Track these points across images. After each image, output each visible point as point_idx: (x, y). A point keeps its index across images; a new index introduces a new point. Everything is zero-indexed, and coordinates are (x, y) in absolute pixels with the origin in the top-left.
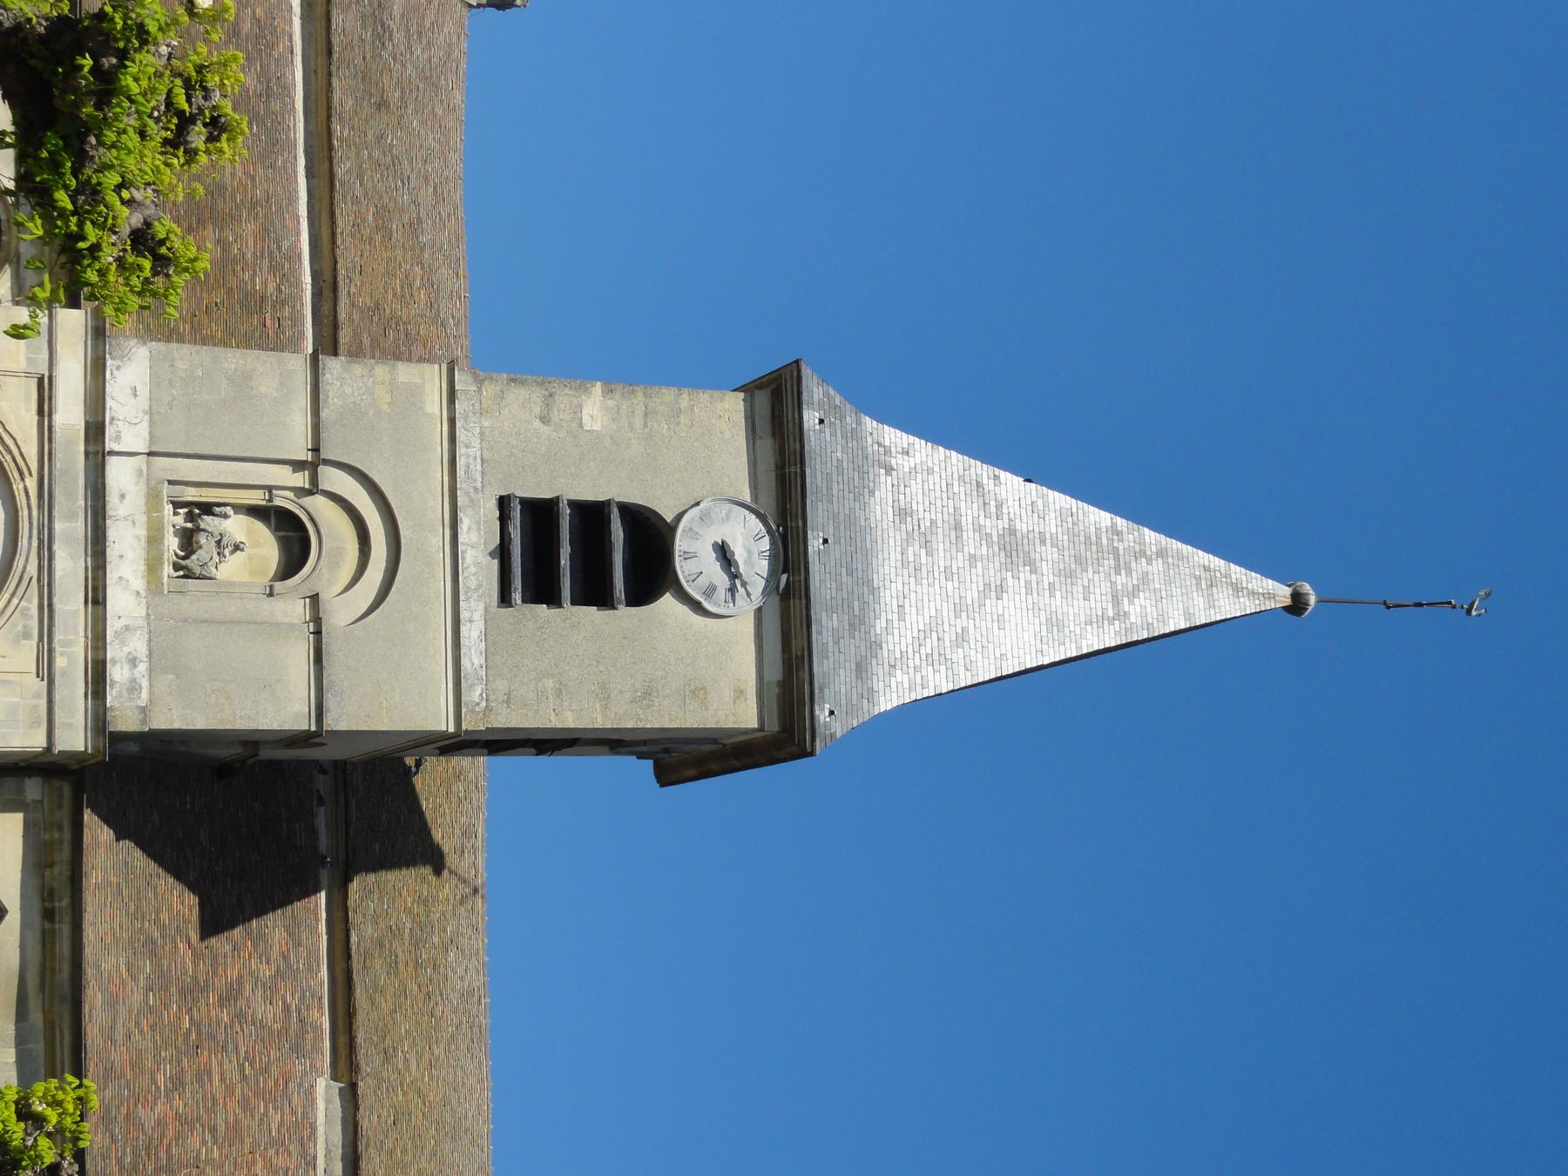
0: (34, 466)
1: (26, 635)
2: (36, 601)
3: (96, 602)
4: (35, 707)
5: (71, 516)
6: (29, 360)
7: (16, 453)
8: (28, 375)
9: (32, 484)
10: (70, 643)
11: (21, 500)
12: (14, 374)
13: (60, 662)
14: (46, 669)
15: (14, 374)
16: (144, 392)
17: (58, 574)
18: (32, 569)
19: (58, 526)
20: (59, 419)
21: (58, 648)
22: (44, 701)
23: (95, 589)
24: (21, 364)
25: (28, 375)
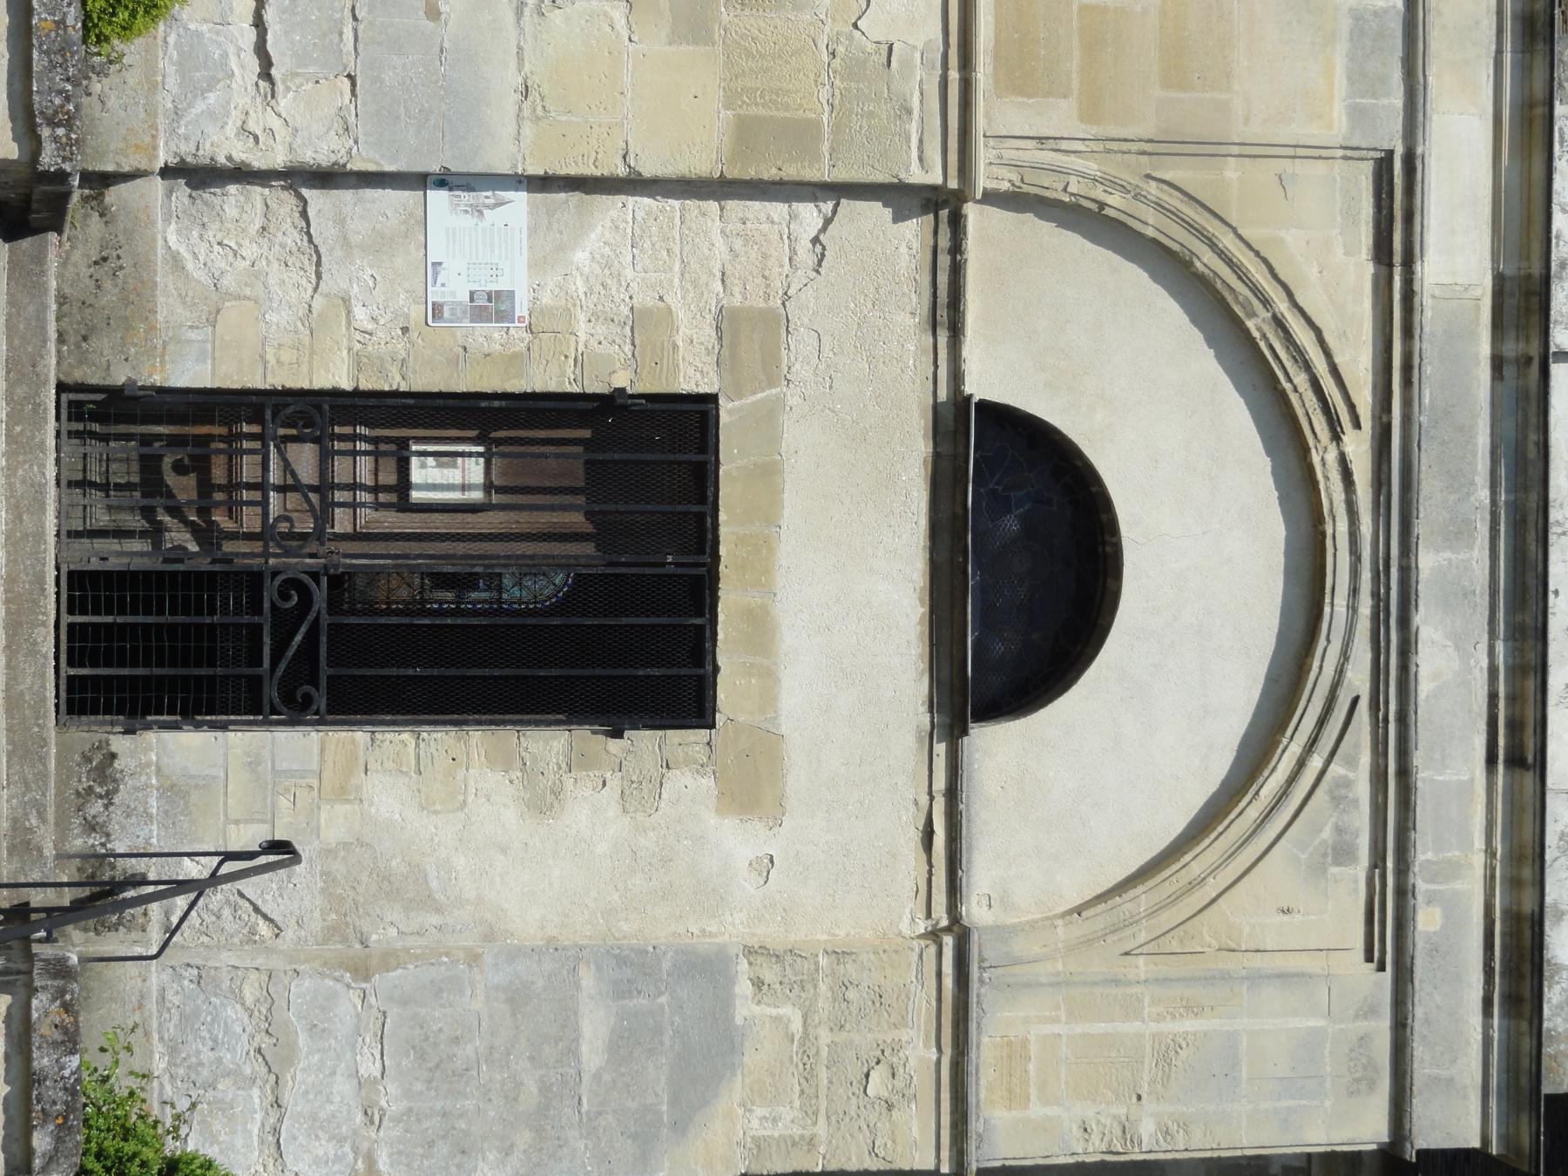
0: (1365, 401)
1: (1343, 853)
2: (1365, 759)
3: (1516, 761)
4: (1364, 1039)
5: (1457, 534)
6: (1357, 114)
7: (1321, 367)
8: (1351, 152)
9: (1358, 447)
10: (1452, 870)
12: (1317, 152)
13: (1427, 920)
14: (1390, 938)
15: (1317, 152)
17: (1425, 687)
18: (1358, 678)
19: (1427, 561)
20: (1433, 271)
21: (1421, 885)
22: (1383, 1026)
23: (1515, 726)
24: (1336, 126)
25: (1351, 152)
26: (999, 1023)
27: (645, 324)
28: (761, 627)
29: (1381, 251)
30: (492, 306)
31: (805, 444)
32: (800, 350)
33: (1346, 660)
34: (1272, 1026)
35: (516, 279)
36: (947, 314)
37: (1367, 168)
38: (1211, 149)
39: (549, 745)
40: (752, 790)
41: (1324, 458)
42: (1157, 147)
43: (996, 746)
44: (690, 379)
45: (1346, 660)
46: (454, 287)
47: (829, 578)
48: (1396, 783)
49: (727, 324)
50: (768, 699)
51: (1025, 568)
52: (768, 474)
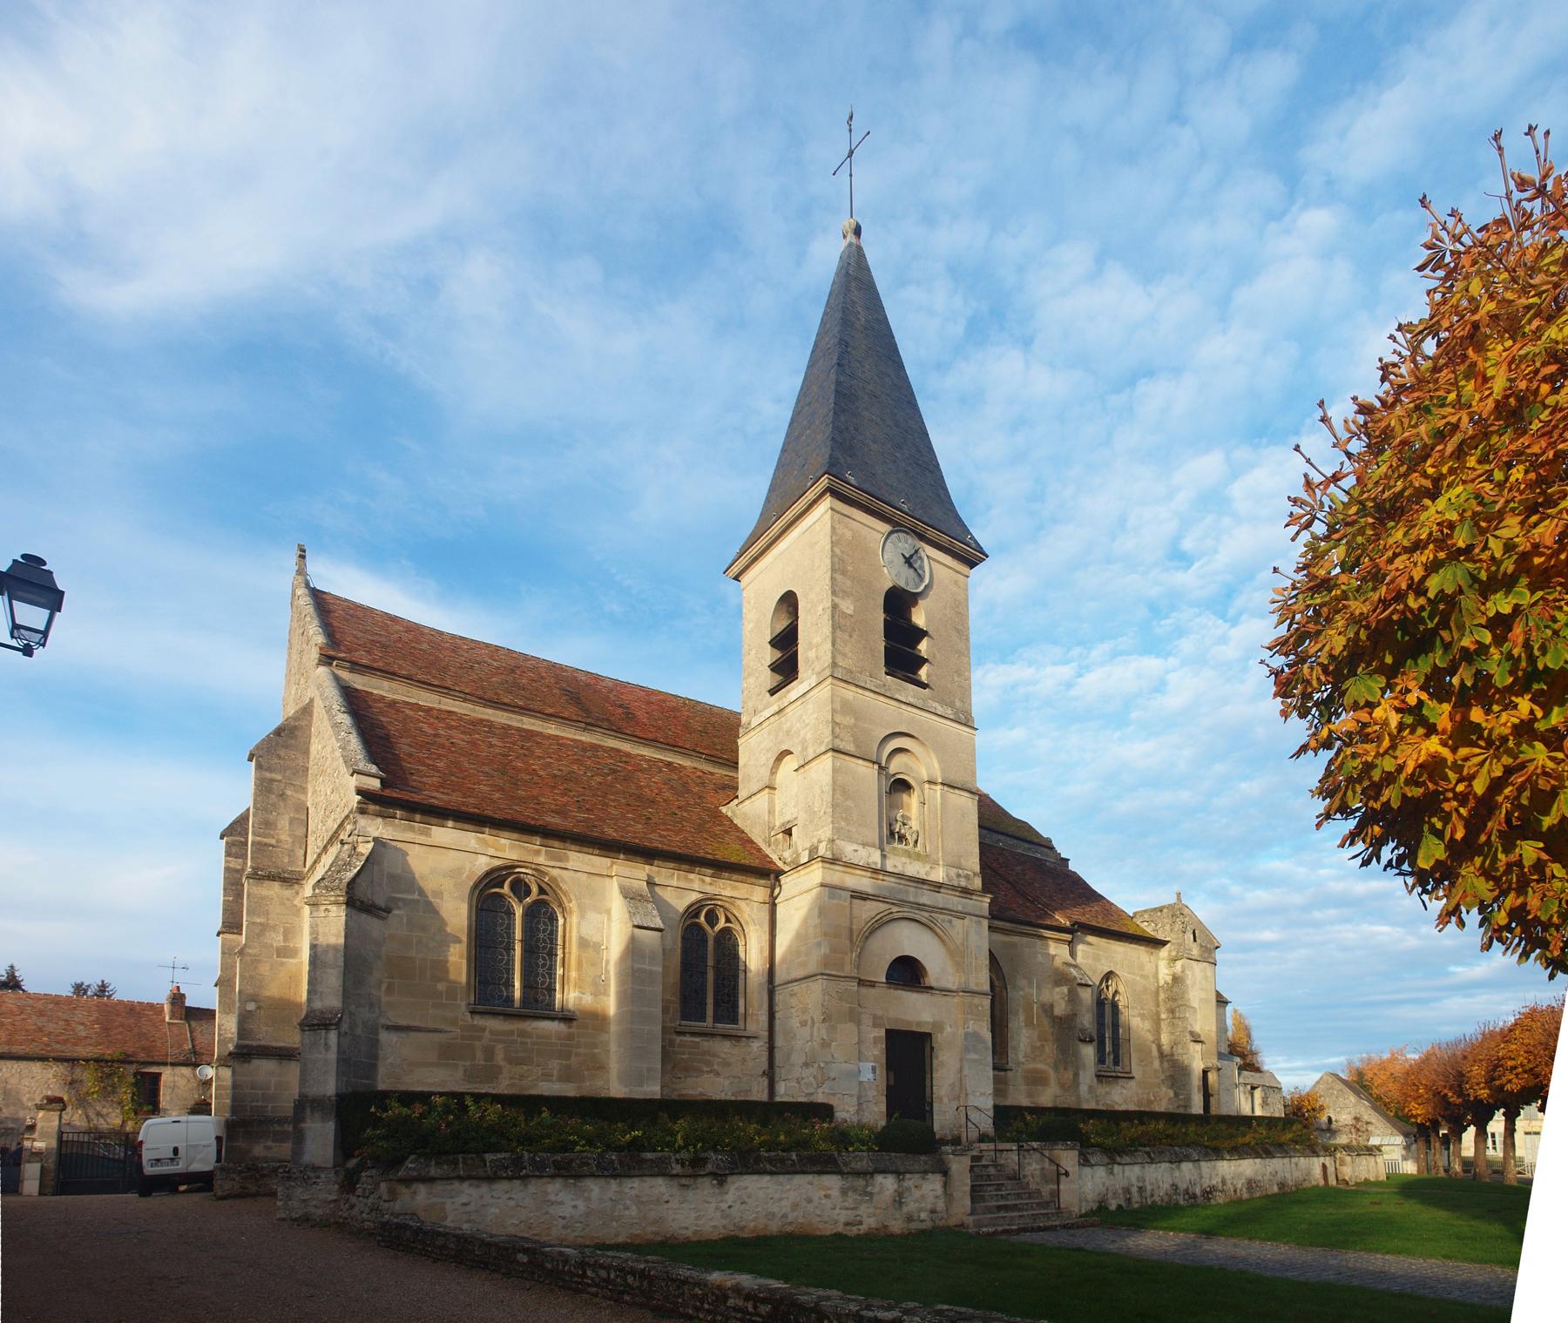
9: (895, 909)
13: (960, 908)
14: (961, 915)
16: (855, 847)
20: (870, 891)
26: (973, 987)
28: (919, 1024)
30: (874, 1069)
32: (879, 1013)
33: (923, 916)
34: (973, 937)
36: (872, 984)
38: (851, 930)
40: (939, 1026)
41: (896, 916)
43: (932, 978)
44: (883, 1033)
45: (923, 916)
46: (871, 1076)
47: (915, 1010)
49: (875, 1025)
51: (907, 972)
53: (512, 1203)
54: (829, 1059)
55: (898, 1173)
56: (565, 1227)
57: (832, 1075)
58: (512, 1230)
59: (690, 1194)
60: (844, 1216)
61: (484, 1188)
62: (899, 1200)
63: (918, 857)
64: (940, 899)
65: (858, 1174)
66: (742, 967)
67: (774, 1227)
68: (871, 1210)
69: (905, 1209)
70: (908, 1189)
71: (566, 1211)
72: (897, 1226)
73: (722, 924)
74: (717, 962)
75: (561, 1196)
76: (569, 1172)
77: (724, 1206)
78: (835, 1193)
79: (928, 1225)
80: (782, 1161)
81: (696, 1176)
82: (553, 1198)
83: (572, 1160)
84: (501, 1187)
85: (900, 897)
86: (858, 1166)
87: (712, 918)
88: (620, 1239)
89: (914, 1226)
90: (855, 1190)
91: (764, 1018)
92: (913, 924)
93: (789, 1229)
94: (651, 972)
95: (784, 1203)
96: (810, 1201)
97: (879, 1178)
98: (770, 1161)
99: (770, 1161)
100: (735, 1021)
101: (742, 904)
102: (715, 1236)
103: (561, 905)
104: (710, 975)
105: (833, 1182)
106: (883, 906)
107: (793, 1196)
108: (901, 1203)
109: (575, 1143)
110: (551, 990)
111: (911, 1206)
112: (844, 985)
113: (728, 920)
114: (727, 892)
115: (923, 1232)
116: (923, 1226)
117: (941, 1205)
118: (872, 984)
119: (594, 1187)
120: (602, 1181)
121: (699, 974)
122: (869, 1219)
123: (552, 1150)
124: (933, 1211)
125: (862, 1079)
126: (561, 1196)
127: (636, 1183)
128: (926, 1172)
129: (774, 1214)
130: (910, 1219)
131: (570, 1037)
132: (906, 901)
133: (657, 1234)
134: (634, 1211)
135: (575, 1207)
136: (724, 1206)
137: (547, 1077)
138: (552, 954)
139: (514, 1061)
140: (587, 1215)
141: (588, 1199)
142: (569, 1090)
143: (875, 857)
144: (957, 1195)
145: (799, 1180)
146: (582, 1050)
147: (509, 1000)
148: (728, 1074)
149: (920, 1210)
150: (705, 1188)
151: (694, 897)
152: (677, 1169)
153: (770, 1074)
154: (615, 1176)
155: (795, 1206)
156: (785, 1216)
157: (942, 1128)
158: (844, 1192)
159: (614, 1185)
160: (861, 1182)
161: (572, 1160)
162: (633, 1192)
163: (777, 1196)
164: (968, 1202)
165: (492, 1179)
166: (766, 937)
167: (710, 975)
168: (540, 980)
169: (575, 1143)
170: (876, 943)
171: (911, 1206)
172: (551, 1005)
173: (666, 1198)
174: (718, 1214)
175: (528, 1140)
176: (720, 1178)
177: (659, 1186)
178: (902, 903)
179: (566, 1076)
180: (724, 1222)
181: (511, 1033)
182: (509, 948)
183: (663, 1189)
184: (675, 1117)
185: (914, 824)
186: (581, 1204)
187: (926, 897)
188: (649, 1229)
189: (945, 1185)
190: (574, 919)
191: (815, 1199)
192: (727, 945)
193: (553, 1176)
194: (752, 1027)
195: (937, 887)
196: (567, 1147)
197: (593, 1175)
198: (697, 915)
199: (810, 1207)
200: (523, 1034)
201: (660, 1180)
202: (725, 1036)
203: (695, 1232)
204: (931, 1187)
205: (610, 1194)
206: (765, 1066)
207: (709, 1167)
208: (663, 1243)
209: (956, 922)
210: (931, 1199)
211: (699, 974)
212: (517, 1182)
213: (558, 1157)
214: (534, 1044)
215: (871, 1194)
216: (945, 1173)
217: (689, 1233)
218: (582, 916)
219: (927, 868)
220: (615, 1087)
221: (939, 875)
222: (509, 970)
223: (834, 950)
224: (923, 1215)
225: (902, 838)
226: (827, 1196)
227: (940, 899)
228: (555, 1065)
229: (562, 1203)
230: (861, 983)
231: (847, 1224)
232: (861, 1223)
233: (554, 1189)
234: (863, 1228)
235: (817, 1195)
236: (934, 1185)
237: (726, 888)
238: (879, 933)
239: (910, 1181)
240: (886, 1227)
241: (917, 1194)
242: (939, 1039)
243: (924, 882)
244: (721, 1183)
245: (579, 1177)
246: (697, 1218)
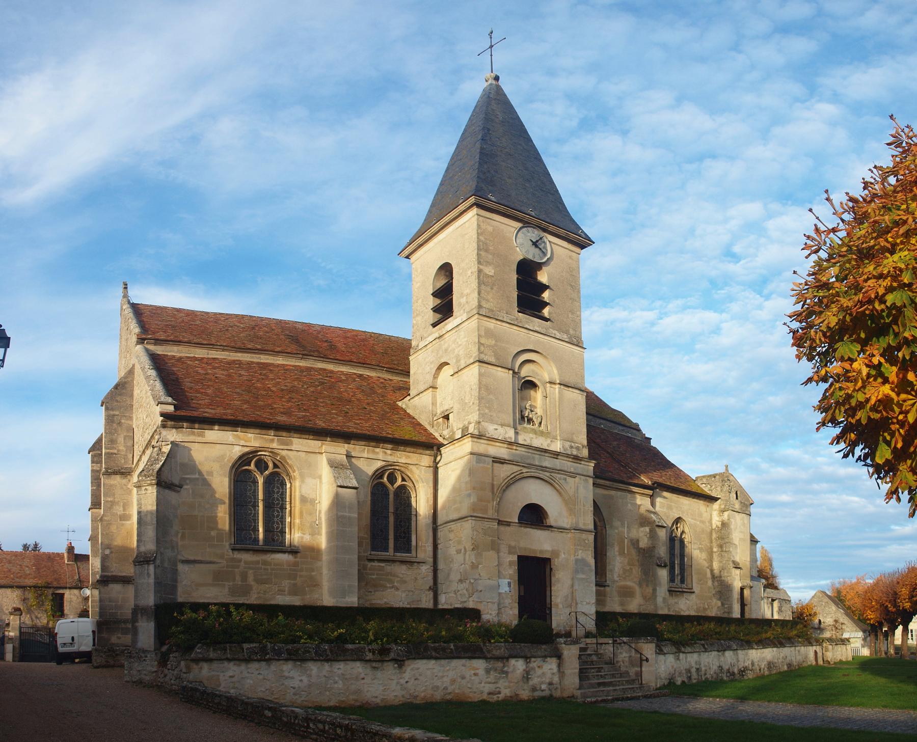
0: (519, 468)
9: (525, 470)
11: (529, 474)
17: (548, 466)
18: (548, 474)
20: (506, 457)
27: (511, 563)
28: (541, 552)
29: (502, 463)
30: (509, 584)
31: (523, 544)
32: (513, 544)
33: (545, 475)
35: (506, 581)
36: (508, 524)
37: (496, 465)
38: (493, 485)
39: (553, 579)
40: (556, 553)
41: (525, 475)
42: (493, 493)
43: (552, 520)
44: (515, 558)
45: (545, 475)
47: (539, 542)
48: (560, 471)
49: (510, 553)
50: (546, 551)
51: (534, 515)
52: (525, 549)
53: (261, 677)
54: (477, 577)
55: (527, 658)
56: (295, 694)
57: (480, 588)
58: (261, 695)
59: (379, 674)
60: (487, 688)
61: (243, 667)
62: (527, 676)
63: (542, 434)
64: (558, 463)
65: (498, 658)
66: (414, 513)
67: (438, 696)
68: (506, 684)
69: (531, 683)
70: (533, 669)
71: (296, 683)
72: (525, 694)
73: (399, 482)
74: (396, 509)
75: (292, 674)
76: (297, 657)
77: (403, 681)
78: (481, 672)
79: (547, 693)
80: (444, 650)
81: (382, 661)
82: (286, 674)
83: (299, 649)
84: (254, 666)
85: (528, 461)
86: (497, 653)
87: (392, 479)
88: (331, 704)
89: (537, 694)
90: (496, 670)
91: (430, 549)
92: (538, 481)
93: (449, 697)
94: (350, 518)
95: (445, 679)
96: (463, 678)
97: (513, 662)
98: (435, 649)
99: (435, 649)
100: (409, 550)
101: (414, 468)
102: (396, 702)
103: (288, 475)
104: (391, 519)
105: (480, 665)
106: (516, 468)
107: (451, 674)
108: (528, 679)
109: (301, 637)
110: (283, 532)
111: (535, 681)
112: (487, 524)
113: (403, 480)
114: (403, 460)
115: (543, 698)
116: (543, 694)
117: (556, 679)
118: (508, 524)
119: (314, 668)
120: (319, 663)
121: (384, 517)
122: (505, 690)
123: (286, 642)
124: (550, 684)
125: (501, 591)
126: (292, 674)
127: (341, 665)
128: (545, 657)
129: (438, 687)
130: (534, 689)
131: (296, 564)
132: (533, 464)
133: (356, 701)
134: (340, 685)
135: (301, 681)
136: (403, 681)
137: (281, 592)
138: (283, 508)
139: (260, 582)
140: (310, 686)
141: (310, 676)
142: (296, 601)
143: (510, 434)
144: (568, 672)
145: (456, 663)
146: (304, 573)
147: (256, 540)
148: (404, 589)
149: (542, 683)
150: (390, 669)
151: (379, 464)
152: (370, 656)
153: (435, 589)
154: (327, 661)
155: (453, 681)
156: (446, 688)
157: (558, 625)
158: (488, 671)
159: (327, 666)
160: (499, 664)
161: (299, 649)
162: (340, 672)
163: (440, 674)
164: (577, 680)
165: (248, 660)
166: (431, 491)
167: (391, 519)
168: (275, 526)
169: (301, 637)
170: (511, 494)
171: (535, 681)
172: (283, 543)
173: (362, 676)
174: (399, 687)
175: (270, 635)
176: (400, 663)
177: (357, 668)
178: (530, 466)
179: (294, 592)
180: (404, 693)
181: (258, 562)
182: (255, 505)
183: (360, 670)
184: (368, 620)
185: (539, 411)
186: (305, 679)
187: (548, 462)
188: (351, 697)
189: (559, 666)
190: (297, 483)
191: (468, 676)
192: (403, 497)
193: (287, 660)
194: (421, 556)
195: (556, 455)
196: (295, 640)
197: (312, 660)
198: (381, 477)
199: (464, 682)
200: (265, 563)
201: (358, 664)
202: (403, 562)
203: (382, 700)
204: (549, 667)
205: (324, 673)
206: (431, 583)
207: (392, 655)
208: (360, 707)
209: (569, 479)
210: (549, 675)
211: (384, 517)
212: (264, 663)
213: (290, 647)
214: (272, 569)
215: (507, 673)
216: (559, 657)
217: (378, 701)
218: (302, 481)
219: (549, 441)
220: (328, 600)
221: (557, 446)
222: (256, 521)
223: (480, 499)
224: (544, 687)
225: (530, 420)
226: (475, 674)
227: (558, 463)
228: (286, 583)
229: (292, 678)
230: (500, 523)
231: (490, 694)
232: (499, 693)
233: (288, 668)
234: (501, 696)
235: (469, 673)
236: (551, 665)
237: (401, 457)
238: (513, 488)
239: (535, 663)
240: (517, 695)
241: (539, 672)
242: (556, 563)
243: (546, 451)
244: (400, 667)
245: (303, 660)
246: (384, 690)
